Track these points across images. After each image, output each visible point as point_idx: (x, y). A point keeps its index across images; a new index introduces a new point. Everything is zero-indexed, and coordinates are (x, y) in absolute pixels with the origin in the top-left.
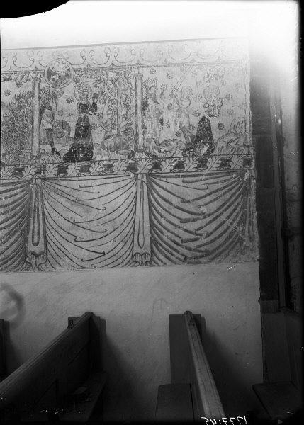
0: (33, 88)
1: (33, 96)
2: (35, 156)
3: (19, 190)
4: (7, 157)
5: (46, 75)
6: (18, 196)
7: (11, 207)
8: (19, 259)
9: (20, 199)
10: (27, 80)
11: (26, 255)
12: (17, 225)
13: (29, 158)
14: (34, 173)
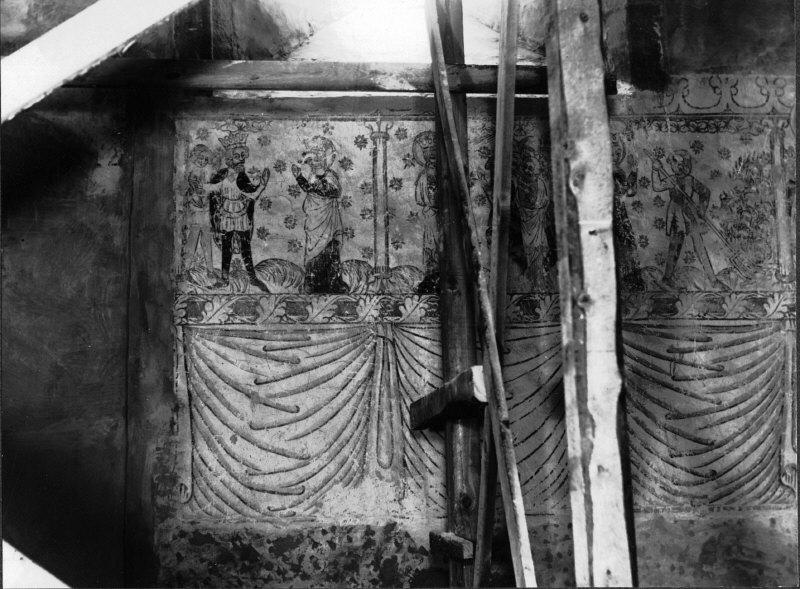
0: (772, 147)
1: (771, 161)
2: (784, 276)
3: (760, 342)
4: (732, 275)
5: (792, 123)
6: (760, 353)
7: (747, 374)
8: (768, 479)
9: (764, 358)
10: (760, 131)
11: (780, 473)
12: (761, 412)
13: (774, 279)
14: (785, 309)
